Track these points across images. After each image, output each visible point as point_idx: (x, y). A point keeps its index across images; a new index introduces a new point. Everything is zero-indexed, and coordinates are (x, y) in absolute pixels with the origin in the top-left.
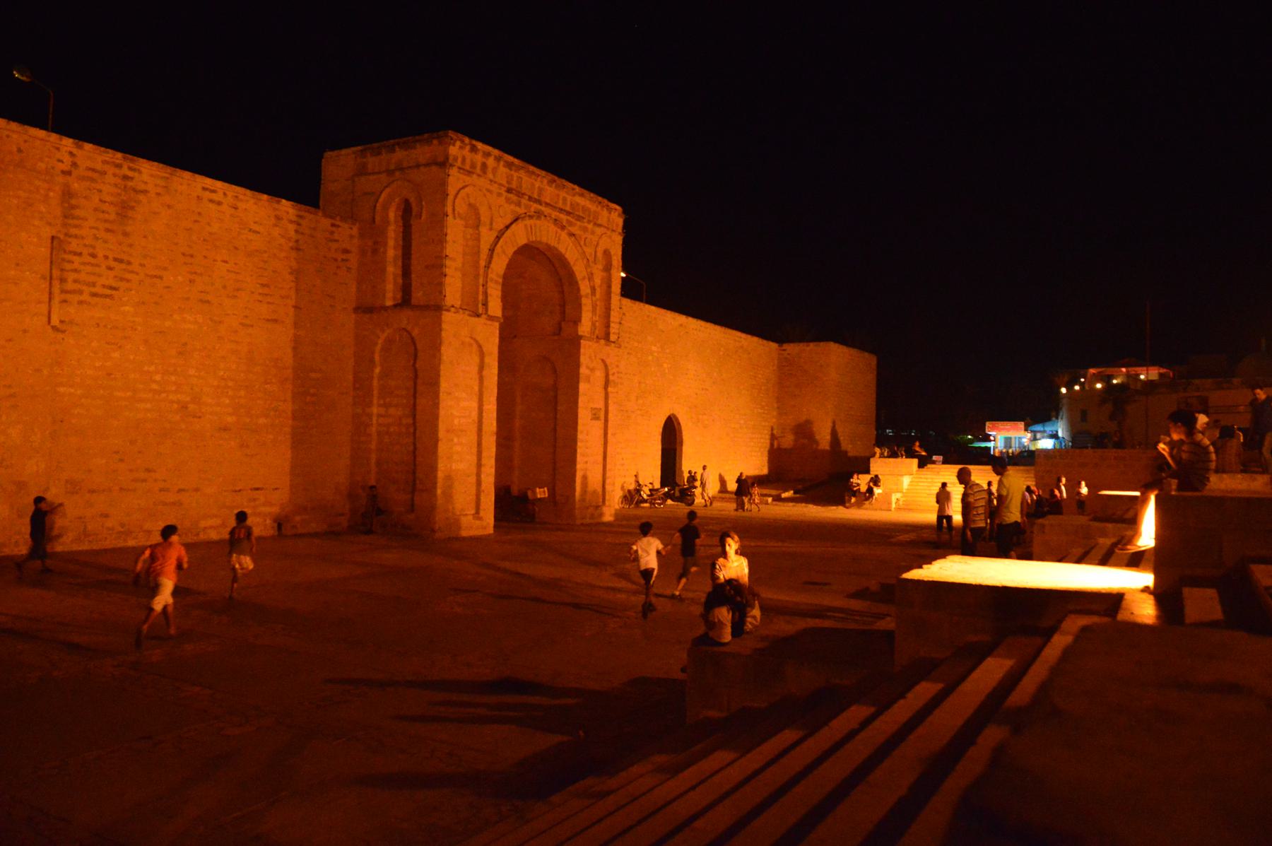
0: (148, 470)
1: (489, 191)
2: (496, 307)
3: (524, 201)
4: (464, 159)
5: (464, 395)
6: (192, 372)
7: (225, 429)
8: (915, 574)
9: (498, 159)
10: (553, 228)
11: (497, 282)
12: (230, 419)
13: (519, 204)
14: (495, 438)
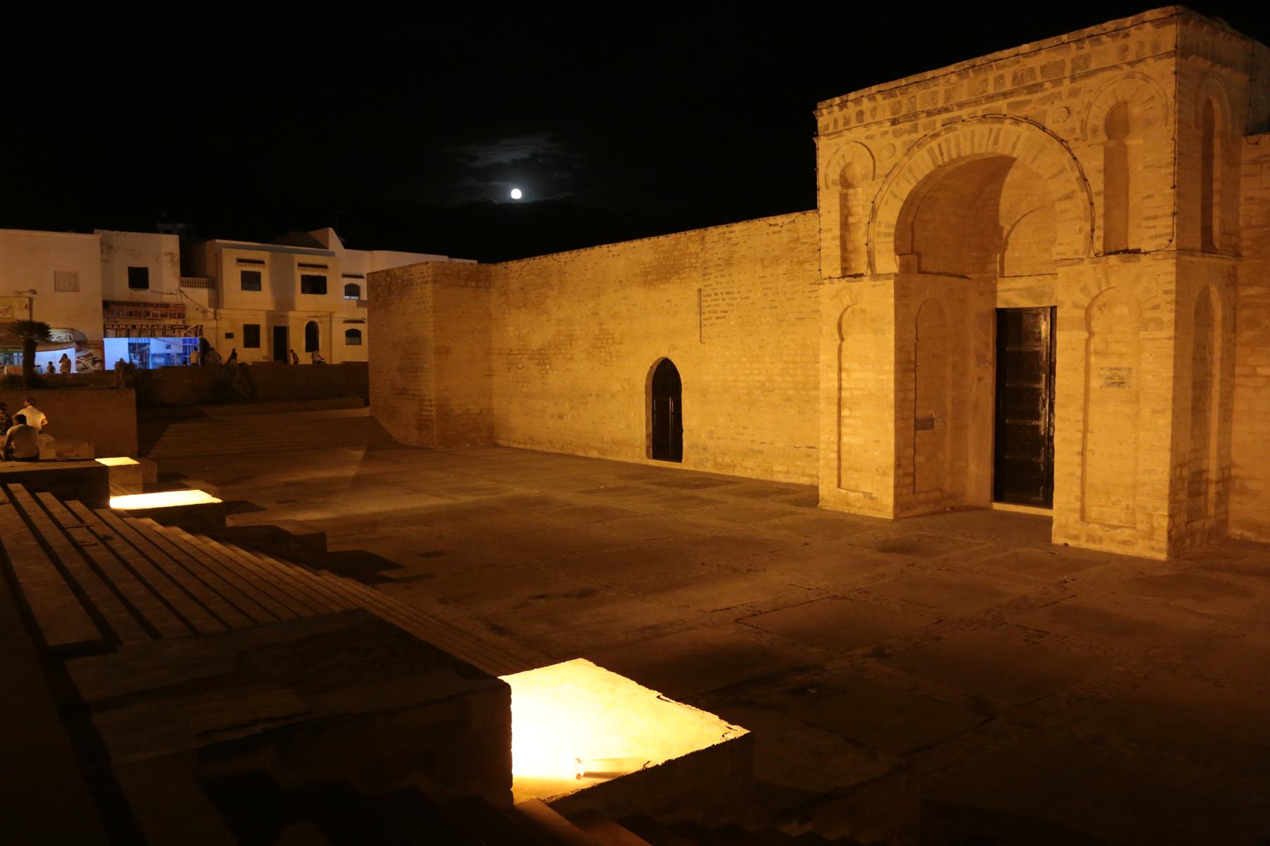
0: (745, 428)
1: (872, 137)
2: (888, 263)
3: (923, 120)
4: (836, 121)
5: (856, 366)
6: (767, 359)
7: (788, 400)
8: (217, 501)
9: (872, 98)
10: (981, 129)
11: (887, 235)
12: (791, 393)
13: (915, 129)
14: (892, 411)
